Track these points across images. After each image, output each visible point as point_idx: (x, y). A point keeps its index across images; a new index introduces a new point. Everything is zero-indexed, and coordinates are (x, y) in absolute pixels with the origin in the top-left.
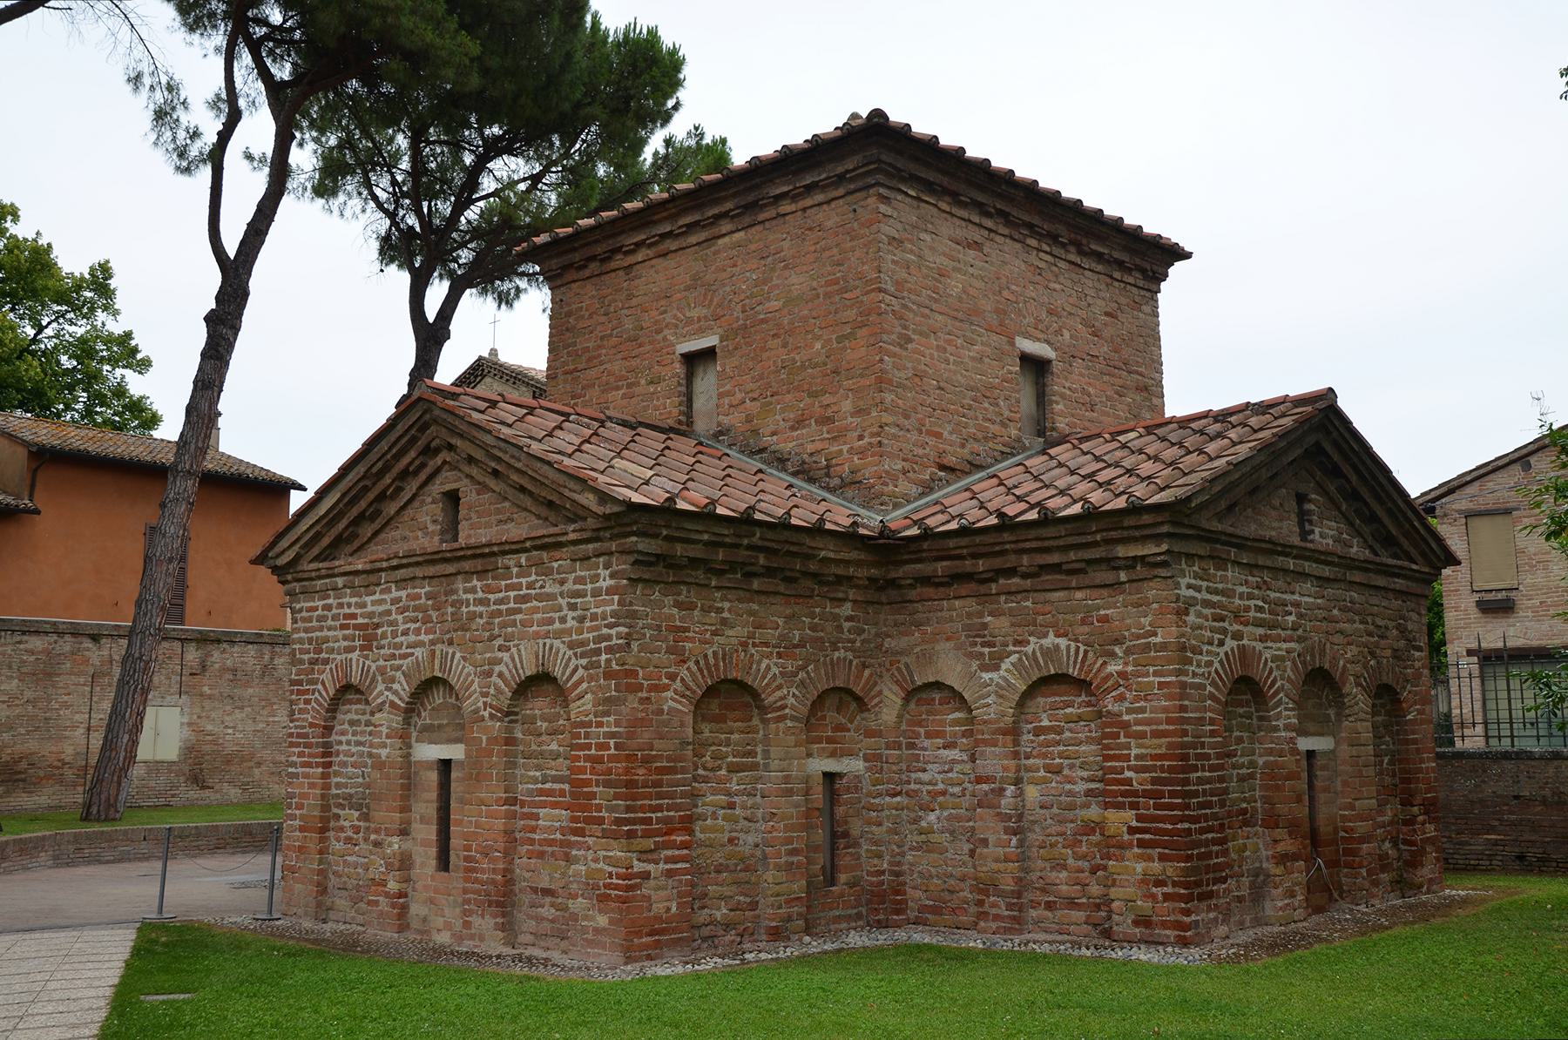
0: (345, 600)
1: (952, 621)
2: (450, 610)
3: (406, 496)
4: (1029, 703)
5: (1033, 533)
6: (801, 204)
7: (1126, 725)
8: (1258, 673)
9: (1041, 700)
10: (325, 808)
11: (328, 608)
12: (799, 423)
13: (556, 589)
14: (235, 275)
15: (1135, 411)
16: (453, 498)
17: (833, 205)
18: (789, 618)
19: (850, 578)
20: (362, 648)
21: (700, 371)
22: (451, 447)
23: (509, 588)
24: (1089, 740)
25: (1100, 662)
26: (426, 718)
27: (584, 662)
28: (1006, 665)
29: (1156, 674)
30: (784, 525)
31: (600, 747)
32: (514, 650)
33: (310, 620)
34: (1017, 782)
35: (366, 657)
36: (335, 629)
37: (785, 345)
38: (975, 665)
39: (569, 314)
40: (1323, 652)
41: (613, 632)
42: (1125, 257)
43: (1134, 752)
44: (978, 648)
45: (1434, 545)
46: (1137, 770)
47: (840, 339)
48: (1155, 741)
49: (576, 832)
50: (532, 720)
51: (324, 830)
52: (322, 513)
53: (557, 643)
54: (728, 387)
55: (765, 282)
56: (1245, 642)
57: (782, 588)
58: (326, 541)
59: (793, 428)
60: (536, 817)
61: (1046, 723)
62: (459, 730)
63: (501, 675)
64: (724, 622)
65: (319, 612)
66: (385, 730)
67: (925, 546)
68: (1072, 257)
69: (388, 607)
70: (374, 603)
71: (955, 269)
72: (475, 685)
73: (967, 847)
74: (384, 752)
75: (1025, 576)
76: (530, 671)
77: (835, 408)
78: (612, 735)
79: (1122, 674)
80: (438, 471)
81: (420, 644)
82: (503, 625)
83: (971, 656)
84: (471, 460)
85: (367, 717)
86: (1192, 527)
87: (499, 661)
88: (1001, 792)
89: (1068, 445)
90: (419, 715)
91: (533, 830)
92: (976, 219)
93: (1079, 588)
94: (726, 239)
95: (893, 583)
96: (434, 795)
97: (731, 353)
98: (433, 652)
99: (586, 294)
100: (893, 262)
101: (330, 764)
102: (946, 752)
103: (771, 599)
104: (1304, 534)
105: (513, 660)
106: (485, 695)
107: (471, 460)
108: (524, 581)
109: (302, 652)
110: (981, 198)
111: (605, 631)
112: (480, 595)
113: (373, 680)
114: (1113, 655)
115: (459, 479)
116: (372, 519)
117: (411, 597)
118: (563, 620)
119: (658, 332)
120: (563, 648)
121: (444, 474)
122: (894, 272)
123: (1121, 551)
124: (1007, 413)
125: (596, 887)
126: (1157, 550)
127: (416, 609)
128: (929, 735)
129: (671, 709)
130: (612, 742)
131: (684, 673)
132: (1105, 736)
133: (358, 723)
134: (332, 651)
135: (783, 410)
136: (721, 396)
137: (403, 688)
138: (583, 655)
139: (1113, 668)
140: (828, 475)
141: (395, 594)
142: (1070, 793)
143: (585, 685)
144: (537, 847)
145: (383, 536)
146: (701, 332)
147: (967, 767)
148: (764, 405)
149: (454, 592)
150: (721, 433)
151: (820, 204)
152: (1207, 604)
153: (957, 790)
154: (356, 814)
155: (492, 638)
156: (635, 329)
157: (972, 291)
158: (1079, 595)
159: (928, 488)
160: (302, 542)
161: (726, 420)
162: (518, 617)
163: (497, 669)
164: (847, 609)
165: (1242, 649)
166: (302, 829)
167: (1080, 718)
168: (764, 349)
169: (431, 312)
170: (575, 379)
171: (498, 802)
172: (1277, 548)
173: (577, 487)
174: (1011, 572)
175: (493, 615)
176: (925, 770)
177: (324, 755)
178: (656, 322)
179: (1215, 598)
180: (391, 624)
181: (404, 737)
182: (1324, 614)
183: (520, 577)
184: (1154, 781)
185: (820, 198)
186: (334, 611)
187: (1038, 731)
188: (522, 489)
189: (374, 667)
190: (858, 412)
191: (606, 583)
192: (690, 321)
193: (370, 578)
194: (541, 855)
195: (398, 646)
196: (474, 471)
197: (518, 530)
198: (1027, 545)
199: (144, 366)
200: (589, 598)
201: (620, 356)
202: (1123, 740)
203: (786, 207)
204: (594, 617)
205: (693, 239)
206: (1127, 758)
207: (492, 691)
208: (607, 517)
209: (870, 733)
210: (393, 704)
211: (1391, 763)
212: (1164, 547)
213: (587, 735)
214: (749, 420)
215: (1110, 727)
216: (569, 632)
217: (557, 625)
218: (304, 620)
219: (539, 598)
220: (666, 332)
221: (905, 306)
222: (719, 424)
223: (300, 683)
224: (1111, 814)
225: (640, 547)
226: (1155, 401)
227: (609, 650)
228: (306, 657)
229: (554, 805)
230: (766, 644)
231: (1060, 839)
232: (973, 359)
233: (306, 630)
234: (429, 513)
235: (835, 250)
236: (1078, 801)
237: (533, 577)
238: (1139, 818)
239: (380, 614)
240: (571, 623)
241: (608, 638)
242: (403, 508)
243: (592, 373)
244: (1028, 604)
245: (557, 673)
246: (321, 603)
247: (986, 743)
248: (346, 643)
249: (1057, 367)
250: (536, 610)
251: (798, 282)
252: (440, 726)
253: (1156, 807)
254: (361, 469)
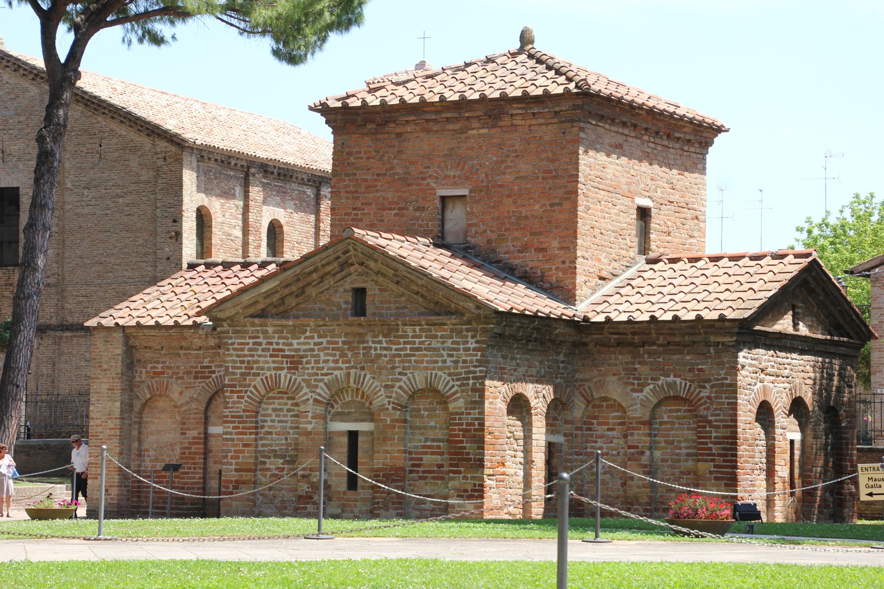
0: (275, 340)
1: (616, 365)
2: (361, 352)
3: (325, 285)
4: (657, 410)
5: (667, 325)
6: (528, 122)
7: (710, 421)
8: (771, 400)
9: (664, 408)
10: (256, 458)
11: (260, 344)
12: (524, 249)
13: (439, 345)
15: (690, 233)
16: (360, 293)
17: (550, 127)
18: (541, 362)
19: (565, 342)
20: (289, 368)
21: (450, 206)
22: (362, 264)
23: (405, 343)
24: (688, 429)
25: (698, 390)
26: (338, 408)
27: (459, 383)
28: (647, 389)
29: (726, 398)
30: (548, 318)
31: (468, 424)
32: (410, 375)
33: (242, 350)
34: (650, 448)
35: (294, 374)
36: (266, 356)
37: (515, 202)
38: (629, 388)
39: (350, 154)
40: (801, 389)
41: (478, 369)
42: (692, 137)
43: (714, 434)
44: (631, 381)
45: (863, 329)
46: (715, 443)
47: (552, 205)
48: (725, 430)
49: (451, 465)
50: (419, 410)
51: (255, 470)
52: (263, 291)
53: (440, 373)
54: (474, 221)
55: (502, 162)
56: (766, 383)
57: (539, 348)
58: (260, 306)
59: (519, 251)
60: (421, 459)
61: (666, 419)
62: (371, 416)
63: (400, 387)
64: (518, 365)
65: (251, 346)
66: (310, 415)
67: (607, 326)
68: (665, 143)
69: (312, 346)
70: (298, 344)
71: (611, 163)
72: (382, 392)
73: (620, 482)
74: (309, 427)
75: (659, 346)
76: (421, 385)
77: (547, 244)
78: (477, 419)
79: (709, 398)
80: (351, 274)
81: (341, 369)
82: (400, 362)
83: (627, 384)
84: (378, 273)
85: (289, 407)
86: (747, 329)
87: (400, 380)
88: (642, 453)
89: (662, 263)
90: (332, 407)
91: (419, 466)
92: (621, 130)
93: (688, 354)
94: (475, 132)
95: (585, 344)
96: (345, 450)
97: (477, 202)
98: (348, 374)
99: (364, 144)
100: (585, 165)
101: (257, 434)
102: (609, 433)
103: (534, 353)
104: (795, 325)
105: (410, 380)
106: (390, 397)
107: (378, 273)
108: (417, 340)
109: (233, 368)
110: (624, 119)
111: (472, 369)
112: (385, 345)
113: (299, 388)
114: (704, 387)
115: (367, 282)
116: (297, 296)
117: (328, 343)
118: (444, 362)
119: (425, 179)
120: (444, 376)
121: (354, 277)
122: (585, 170)
123: (712, 339)
124: (629, 244)
125: (466, 491)
126: (730, 339)
127: (333, 349)
128: (599, 424)
129: (500, 409)
130: (476, 423)
131: (503, 390)
132: (699, 427)
133: (282, 410)
134: (263, 369)
135: (514, 240)
136: (469, 225)
137: (323, 391)
138: (458, 380)
139: (705, 393)
140: (542, 281)
141: (316, 340)
142: (678, 454)
143: (459, 395)
144: (421, 474)
145: (303, 306)
146: (455, 185)
147: (622, 441)
148: (499, 236)
149: (367, 342)
150: (469, 248)
151: (541, 125)
152: (751, 365)
153: (614, 452)
154: (281, 461)
155: (393, 368)
156: (405, 173)
157: (617, 174)
158: (688, 357)
159: (594, 291)
160: (242, 305)
161: (473, 241)
162: (413, 359)
163: (398, 384)
164: (561, 357)
165: (764, 387)
166: (236, 470)
167: (684, 418)
168: (499, 202)
170: (357, 198)
171: (398, 451)
172: (781, 336)
173: (463, 298)
174: (654, 344)
175: (395, 356)
176: (596, 442)
177: (256, 428)
178: (421, 173)
179: (754, 362)
180: (314, 356)
181: (325, 418)
182: (802, 368)
184: (723, 449)
185: (541, 121)
186: (264, 346)
187: (661, 423)
188: (417, 293)
189: (299, 379)
190: (562, 248)
191: (472, 344)
192: (447, 177)
194: (424, 478)
195: (318, 369)
196: (380, 279)
198: (663, 331)
200: (461, 352)
201: (392, 189)
202: (708, 429)
203: (518, 121)
204: (465, 362)
205: (451, 127)
206: (710, 437)
207: (394, 395)
208: (479, 316)
209: (566, 422)
210: (315, 400)
211: (831, 449)
212: (735, 338)
213: (460, 419)
214: (489, 242)
215: (702, 422)
216: (449, 368)
217: (440, 364)
218: (234, 349)
219: (426, 349)
220: (429, 180)
221: (588, 189)
222: (467, 242)
223: (235, 386)
224: (700, 464)
225: (495, 330)
226: (702, 225)
227: (473, 378)
228: (238, 371)
229: (433, 453)
230: (532, 376)
231: (672, 477)
232: (616, 214)
233: (238, 356)
235: (550, 155)
236: (682, 458)
237: (424, 339)
238: (715, 466)
239: (304, 351)
240: (449, 364)
241: (475, 372)
242: (321, 293)
243: (371, 195)
244: (661, 360)
245: (440, 387)
246: (251, 341)
247: (634, 429)
248: (275, 365)
249: (654, 212)
250: (426, 356)
251: (524, 167)
252: (349, 413)
253: (724, 461)
254: (298, 269)
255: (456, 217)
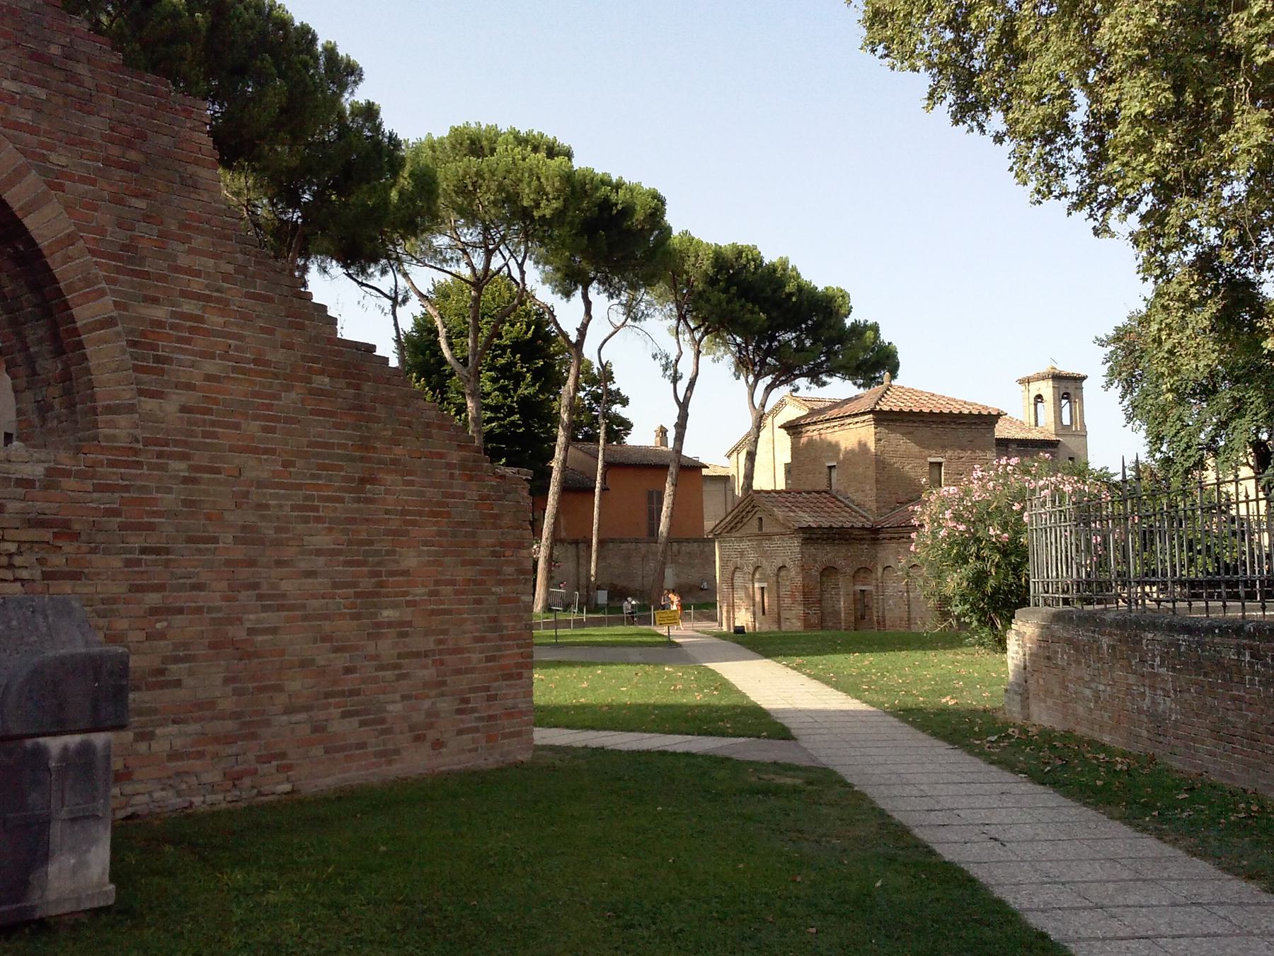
12: (857, 491)
14: (683, 406)
30: (842, 527)
169: (757, 403)
183: (777, 541)
193: (741, 539)
197: (776, 530)
199: (625, 402)
234: (755, 522)
255: (834, 474)
